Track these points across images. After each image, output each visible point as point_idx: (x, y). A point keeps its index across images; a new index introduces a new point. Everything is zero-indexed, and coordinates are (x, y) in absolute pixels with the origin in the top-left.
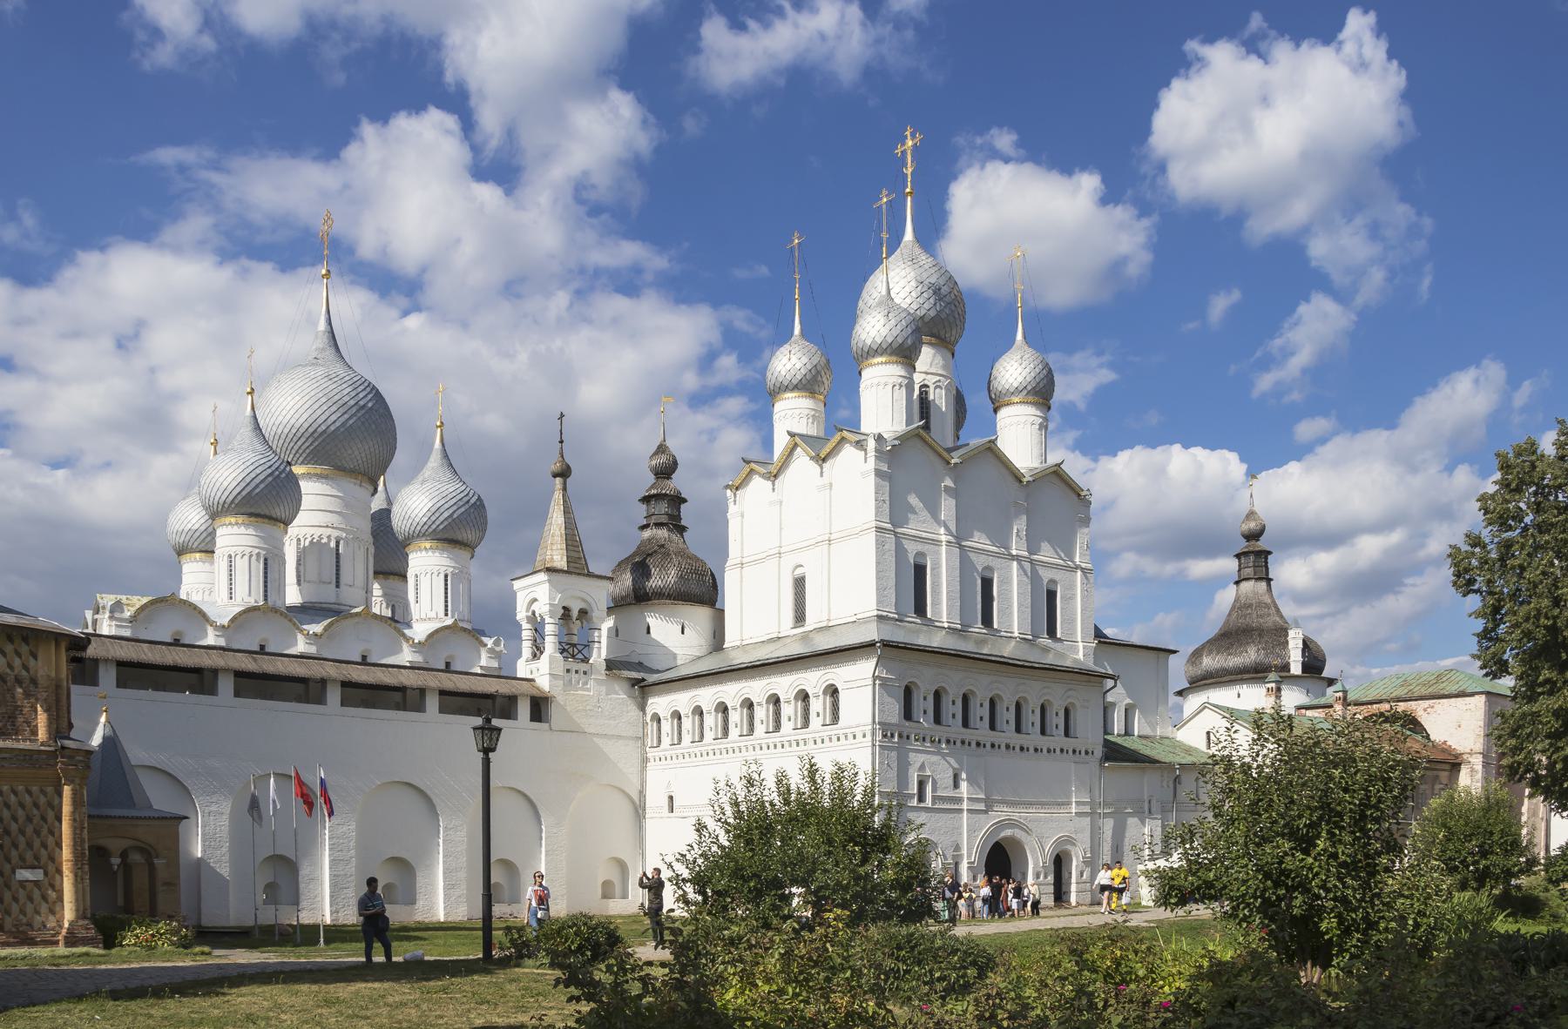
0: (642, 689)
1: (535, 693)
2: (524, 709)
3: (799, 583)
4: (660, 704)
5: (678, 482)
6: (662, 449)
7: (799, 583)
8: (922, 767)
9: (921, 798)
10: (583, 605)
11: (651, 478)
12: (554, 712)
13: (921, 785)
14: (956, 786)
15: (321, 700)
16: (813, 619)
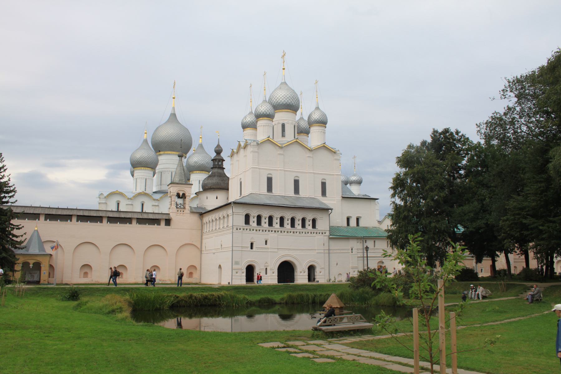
0: (202, 215)
1: (167, 218)
2: (163, 223)
3: (241, 183)
4: (207, 219)
5: (222, 154)
6: (218, 146)
7: (241, 183)
8: (252, 238)
9: (252, 248)
10: (183, 192)
11: (215, 154)
12: (172, 223)
13: (252, 244)
14: (266, 244)
15: (101, 222)
16: (243, 195)
